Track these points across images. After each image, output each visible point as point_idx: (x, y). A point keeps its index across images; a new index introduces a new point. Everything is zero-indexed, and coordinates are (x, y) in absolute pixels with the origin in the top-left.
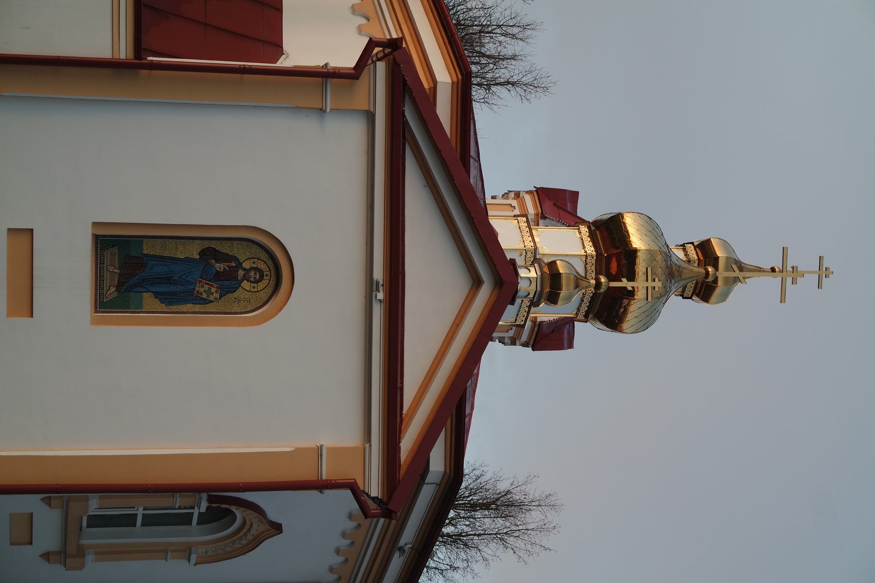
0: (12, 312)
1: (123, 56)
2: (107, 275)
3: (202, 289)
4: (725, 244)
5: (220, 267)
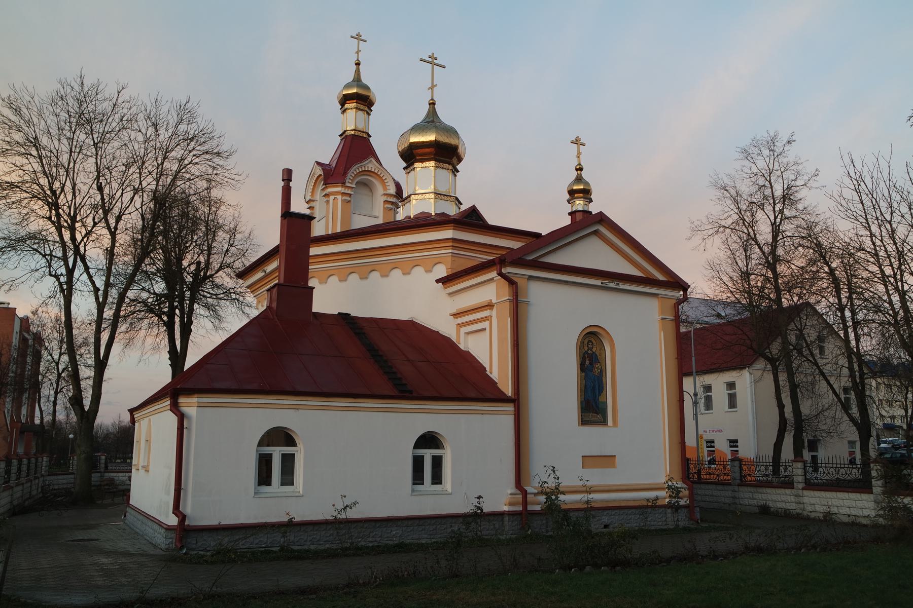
0: (613, 465)
1: (513, 409)
2: (593, 419)
3: (597, 371)
4: (347, 86)
5: (587, 362)
